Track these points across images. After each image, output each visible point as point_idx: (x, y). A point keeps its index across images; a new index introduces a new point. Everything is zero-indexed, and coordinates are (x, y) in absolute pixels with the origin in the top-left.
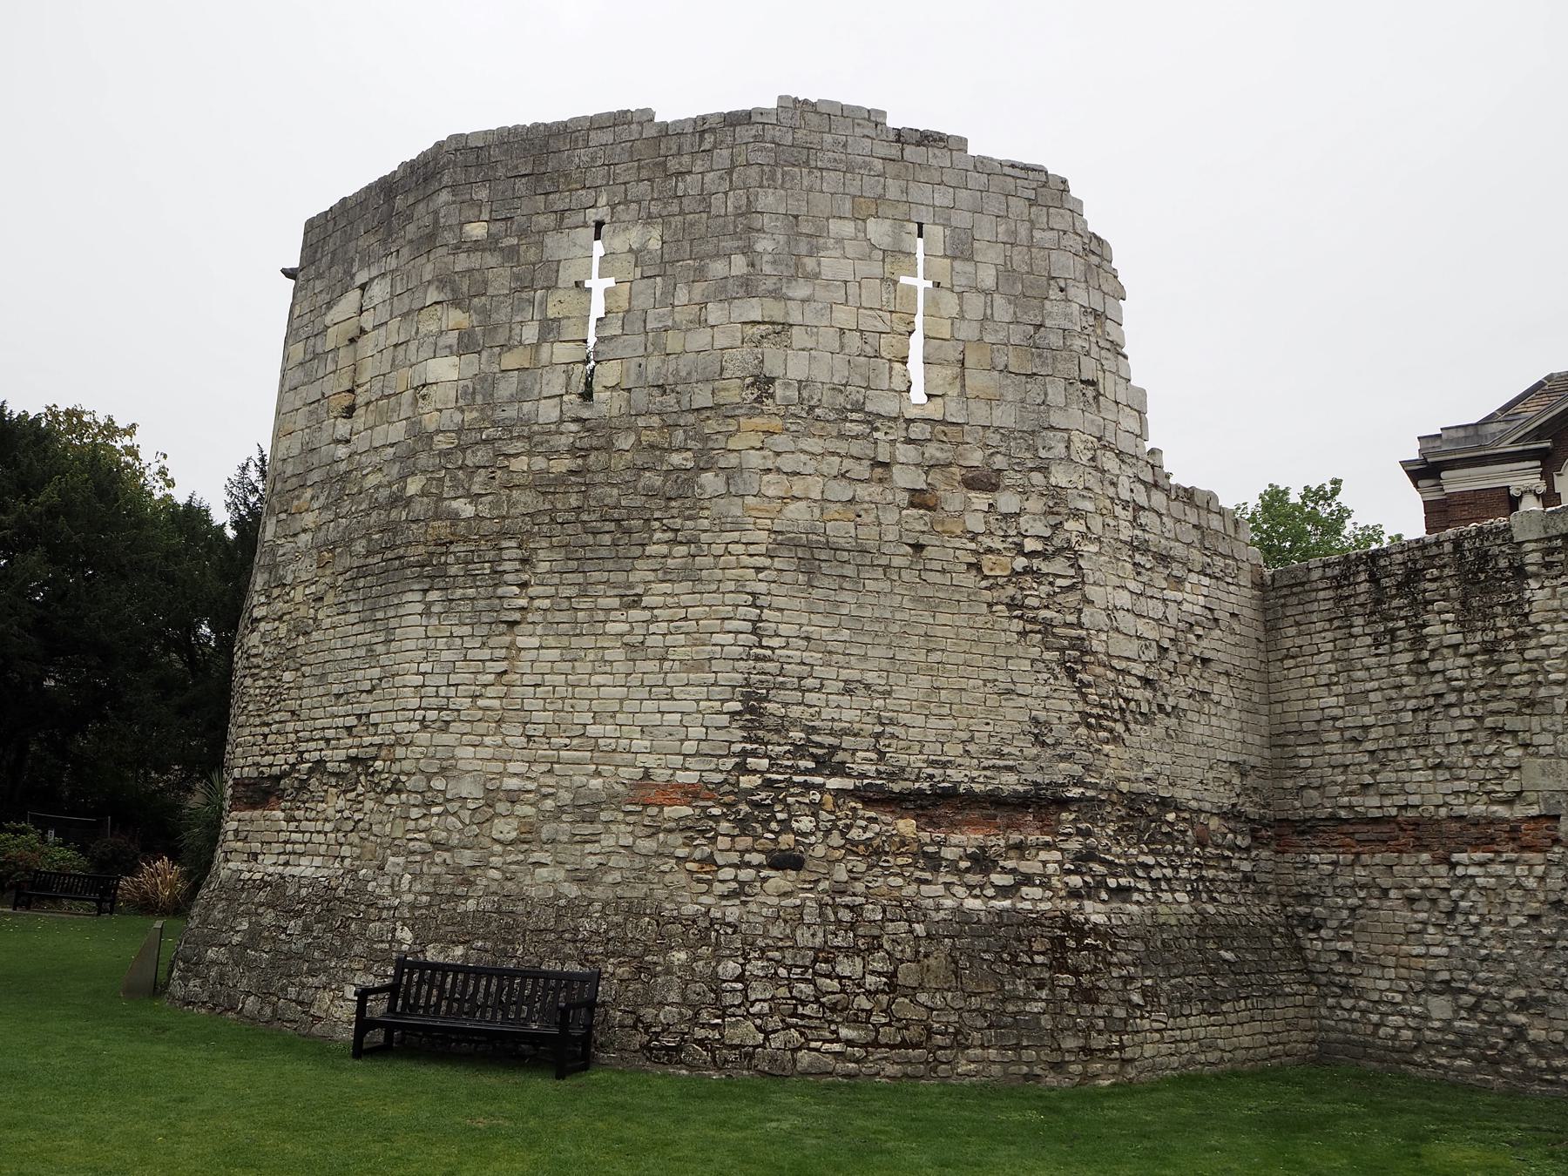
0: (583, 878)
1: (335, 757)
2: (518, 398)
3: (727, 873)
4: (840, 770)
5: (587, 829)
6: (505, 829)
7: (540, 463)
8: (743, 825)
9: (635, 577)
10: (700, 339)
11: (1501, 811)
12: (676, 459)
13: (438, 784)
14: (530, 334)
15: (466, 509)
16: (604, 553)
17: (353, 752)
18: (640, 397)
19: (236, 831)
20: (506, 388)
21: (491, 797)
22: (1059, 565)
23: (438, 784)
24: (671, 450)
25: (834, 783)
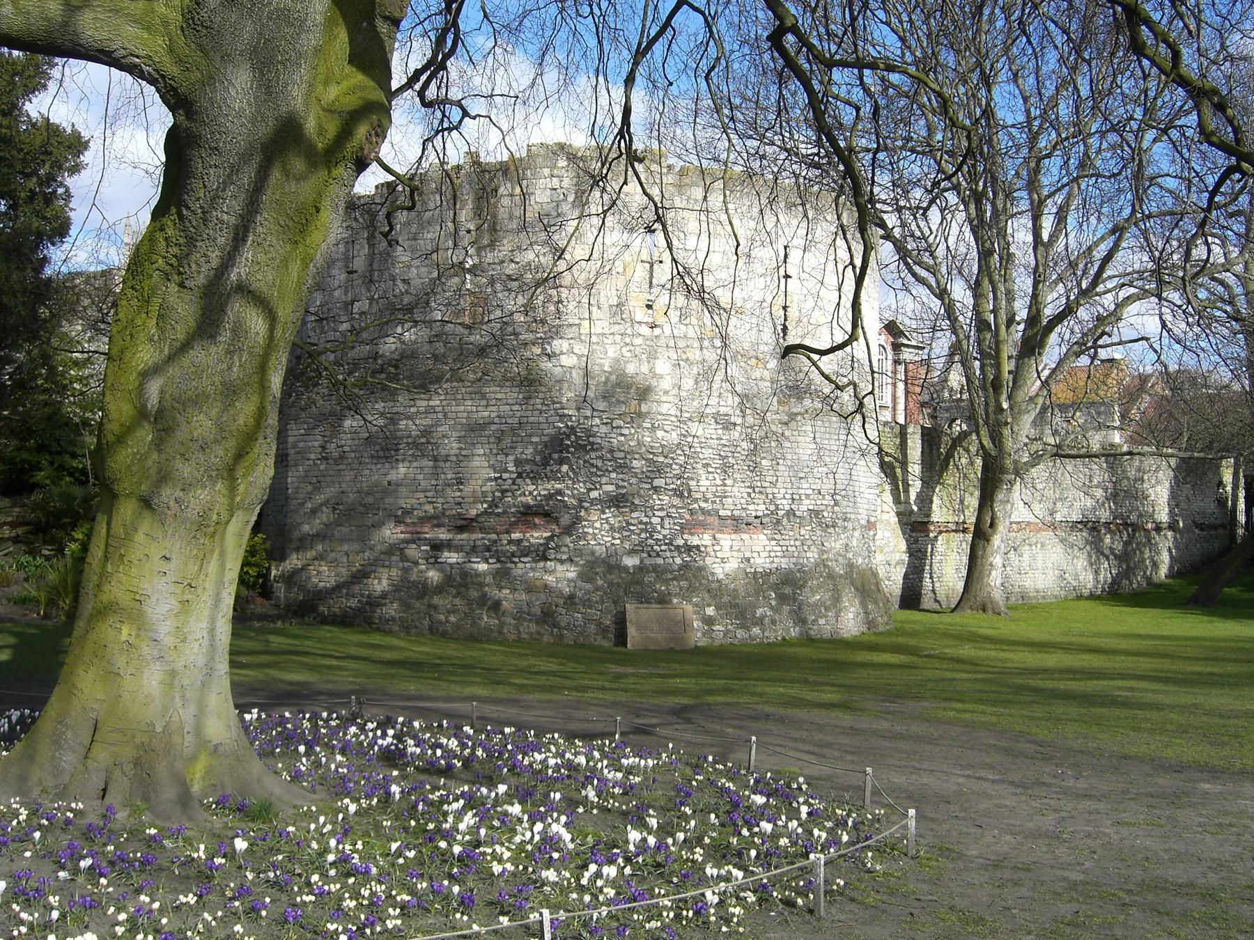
17: (811, 507)
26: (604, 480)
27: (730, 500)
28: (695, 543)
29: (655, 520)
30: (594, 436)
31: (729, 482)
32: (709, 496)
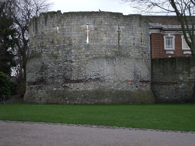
0: (123, 89)
1: (94, 78)
2: (112, 43)
3: (134, 88)
4: (139, 79)
5: (123, 85)
6: (116, 85)
7: (115, 50)
8: (135, 84)
9: (125, 62)
10: (129, 39)
11: (173, 81)
12: (128, 51)
13: (109, 81)
14: (113, 36)
15: (109, 54)
16: (122, 59)
18: (124, 44)
19: (74, 86)
20: (111, 41)
21: (114, 82)
22: (148, 61)
23: (109, 81)
24: (127, 50)
25: (139, 80)
26: (50, 74)
27: (73, 77)
28: (66, 85)
29: (59, 81)
30: (48, 66)
31: (72, 73)
32: (68, 76)
